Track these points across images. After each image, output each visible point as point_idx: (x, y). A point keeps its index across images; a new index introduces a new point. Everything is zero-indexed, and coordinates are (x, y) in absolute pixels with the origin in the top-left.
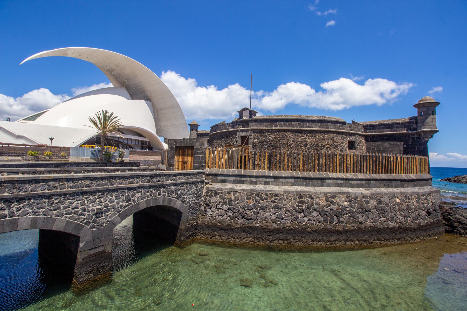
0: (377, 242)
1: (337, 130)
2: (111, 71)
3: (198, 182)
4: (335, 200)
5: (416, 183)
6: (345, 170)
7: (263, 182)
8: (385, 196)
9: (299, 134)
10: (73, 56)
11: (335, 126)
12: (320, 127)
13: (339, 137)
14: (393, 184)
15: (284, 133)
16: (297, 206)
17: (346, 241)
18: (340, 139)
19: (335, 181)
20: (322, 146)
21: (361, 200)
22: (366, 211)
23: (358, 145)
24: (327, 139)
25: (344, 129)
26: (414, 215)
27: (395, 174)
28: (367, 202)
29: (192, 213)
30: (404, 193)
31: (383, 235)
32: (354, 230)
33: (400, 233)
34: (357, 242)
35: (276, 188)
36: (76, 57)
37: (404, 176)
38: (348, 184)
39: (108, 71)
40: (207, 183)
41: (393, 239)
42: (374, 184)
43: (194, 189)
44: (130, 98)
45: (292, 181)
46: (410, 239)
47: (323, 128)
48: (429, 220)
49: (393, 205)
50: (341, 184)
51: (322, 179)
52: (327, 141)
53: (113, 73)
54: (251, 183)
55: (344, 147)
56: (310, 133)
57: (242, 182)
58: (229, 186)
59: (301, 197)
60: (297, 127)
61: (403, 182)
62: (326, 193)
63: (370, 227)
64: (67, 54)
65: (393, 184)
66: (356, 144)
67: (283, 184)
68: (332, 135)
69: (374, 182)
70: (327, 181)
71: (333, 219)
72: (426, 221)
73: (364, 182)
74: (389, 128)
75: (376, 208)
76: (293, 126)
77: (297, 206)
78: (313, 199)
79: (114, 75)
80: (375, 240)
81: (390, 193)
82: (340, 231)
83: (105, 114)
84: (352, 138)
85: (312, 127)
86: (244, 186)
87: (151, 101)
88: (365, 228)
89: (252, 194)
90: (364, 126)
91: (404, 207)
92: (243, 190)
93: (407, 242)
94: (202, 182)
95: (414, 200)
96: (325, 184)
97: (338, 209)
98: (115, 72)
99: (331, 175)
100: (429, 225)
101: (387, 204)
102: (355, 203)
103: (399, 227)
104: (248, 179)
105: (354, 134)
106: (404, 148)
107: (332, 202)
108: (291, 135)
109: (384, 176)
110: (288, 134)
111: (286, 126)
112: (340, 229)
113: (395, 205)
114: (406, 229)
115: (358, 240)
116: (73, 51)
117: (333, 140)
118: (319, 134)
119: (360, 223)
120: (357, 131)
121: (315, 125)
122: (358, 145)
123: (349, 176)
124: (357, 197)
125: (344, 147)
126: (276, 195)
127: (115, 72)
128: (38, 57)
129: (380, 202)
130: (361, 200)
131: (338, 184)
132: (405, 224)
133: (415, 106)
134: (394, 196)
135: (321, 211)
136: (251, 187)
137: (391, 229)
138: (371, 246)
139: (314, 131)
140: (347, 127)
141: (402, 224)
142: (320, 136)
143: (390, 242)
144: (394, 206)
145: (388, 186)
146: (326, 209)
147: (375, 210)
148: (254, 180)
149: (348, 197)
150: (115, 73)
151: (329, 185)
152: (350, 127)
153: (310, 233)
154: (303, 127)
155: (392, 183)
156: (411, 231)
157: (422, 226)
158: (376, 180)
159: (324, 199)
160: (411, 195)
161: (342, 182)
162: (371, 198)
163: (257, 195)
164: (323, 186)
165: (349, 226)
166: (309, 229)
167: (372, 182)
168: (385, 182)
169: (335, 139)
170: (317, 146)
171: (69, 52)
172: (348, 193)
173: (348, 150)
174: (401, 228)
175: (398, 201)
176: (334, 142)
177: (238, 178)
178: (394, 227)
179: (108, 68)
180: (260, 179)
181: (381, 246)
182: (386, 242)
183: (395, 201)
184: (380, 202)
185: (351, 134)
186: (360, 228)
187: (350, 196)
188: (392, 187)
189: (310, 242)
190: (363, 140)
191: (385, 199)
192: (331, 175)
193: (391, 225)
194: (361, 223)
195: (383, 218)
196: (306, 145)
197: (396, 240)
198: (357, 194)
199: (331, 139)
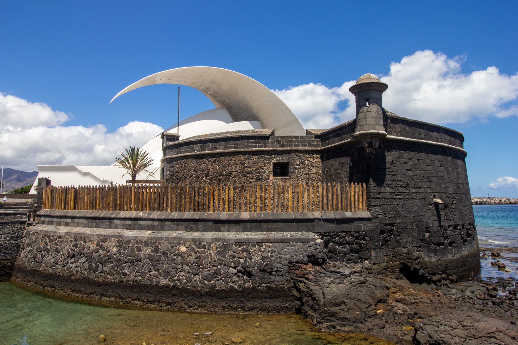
0: (137, 302)
1: (250, 149)
2: (206, 90)
3: (14, 223)
4: (105, 245)
5: (270, 225)
7: (64, 223)
8: (166, 243)
9: (200, 161)
10: (162, 82)
11: (248, 143)
12: (225, 148)
13: (255, 159)
14: (200, 226)
15: (185, 160)
16: (71, 249)
17: (102, 295)
18: (257, 163)
19: (123, 222)
20: (227, 175)
21: (133, 245)
22: (134, 261)
23: (296, 169)
24: (234, 164)
25: (266, 146)
26: (206, 273)
27: (211, 212)
28: (139, 250)
29: (4, 253)
30: (199, 239)
31: (147, 295)
32: (113, 283)
33: (174, 295)
34: (113, 299)
35: (63, 230)
36: (166, 83)
37: (224, 215)
38: (137, 226)
39: (204, 90)
40: (30, 225)
41: (159, 302)
42: (170, 226)
43: (8, 229)
44: (231, 119)
45: (84, 221)
46: (186, 307)
47: (230, 148)
48: (238, 282)
49: (174, 255)
50: (130, 225)
51: (111, 219)
52: (234, 167)
53: (209, 93)
55: (264, 173)
56: (213, 157)
59: (76, 240)
60: (198, 150)
61: (218, 224)
62: (99, 236)
63: (133, 282)
64: (156, 81)
65: (200, 226)
66: (291, 169)
68: (242, 158)
69: (169, 223)
70: (116, 222)
71: (97, 267)
72: (231, 284)
73: (156, 223)
74: (339, 135)
75: (150, 257)
76: (194, 151)
77: (71, 249)
79: (210, 94)
80: (135, 300)
81: (175, 239)
82: (99, 282)
83: (133, 149)
84: (283, 159)
85: (215, 149)
87: (259, 121)
88: (127, 282)
89: (45, 235)
90: (317, 137)
91: (193, 258)
93: (180, 310)
94: (23, 223)
95: (213, 252)
96: (113, 225)
97: (105, 255)
98: (212, 91)
99: (123, 214)
100: (236, 291)
101: (164, 253)
102: (125, 249)
103: (174, 286)
105: (289, 152)
106: (350, 167)
107: (102, 247)
108: (192, 162)
109: (188, 215)
110: (189, 161)
111: (188, 152)
112: (100, 280)
113: (177, 255)
114: (186, 291)
115: (114, 296)
116: (161, 76)
117: (243, 164)
118: (223, 158)
119: (123, 275)
120: (296, 146)
121: (220, 146)
122: (296, 169)
123: (141, 214)
124: (129, 242)
125: (264, 173)
126: (60, 237)
127: (212, 91)
128: (127, 92)
129: (157, 250)
130: (133, 245)
131: (125, 225)
132: (185, 283)
134: (179, 242)
135: (90, 258)
137: (162, 287)
138: (127, 306)
139: (217, 154)
140: (272, 143)
141: (181, 283)
142: (224, 160)
143: (152, 306)
144: (175, 257)
145: (192, 229)
146: (95, 255)
147: (148, 260)
149: (119, 241)
150: (211, 92)
152: (278, 142)
153: (73, 281)
154: (205, 150)
155: (197, 225)
156: (193, 295)
157: (218, 291)
158: (172, 220)
159: (95, 243)
160: (209, 243)
161: (129, 222)
162: (146, 244)
164: (110, 228)
165: (111, 277)
166: (73, 278)
167: (167, 223)
168: (186, 224)
169: (246, 163)
170: (221, 175)
171: (157, 78)
173: (271, 177)
174: (177, 289)
175: (183, 249)
176: (245, 167)
178: (166, 286)
179: (202, 87)
181: (141, 308)
182: (149, 305)
183: (178, 249)
184: (157, 250)
185: (280, 153)
186: (122, 282)
187: (121, 241)
188: (197, 230)
189: (69, 292)
190: (317, 159)
191: (164, 247)
192: (123, 214)
193: (164, 282)
194: (125, 275)
195: (154, 272)
196: (207, 175)
197: (164, 305)
198: (130, 238)
199: (240, 163)
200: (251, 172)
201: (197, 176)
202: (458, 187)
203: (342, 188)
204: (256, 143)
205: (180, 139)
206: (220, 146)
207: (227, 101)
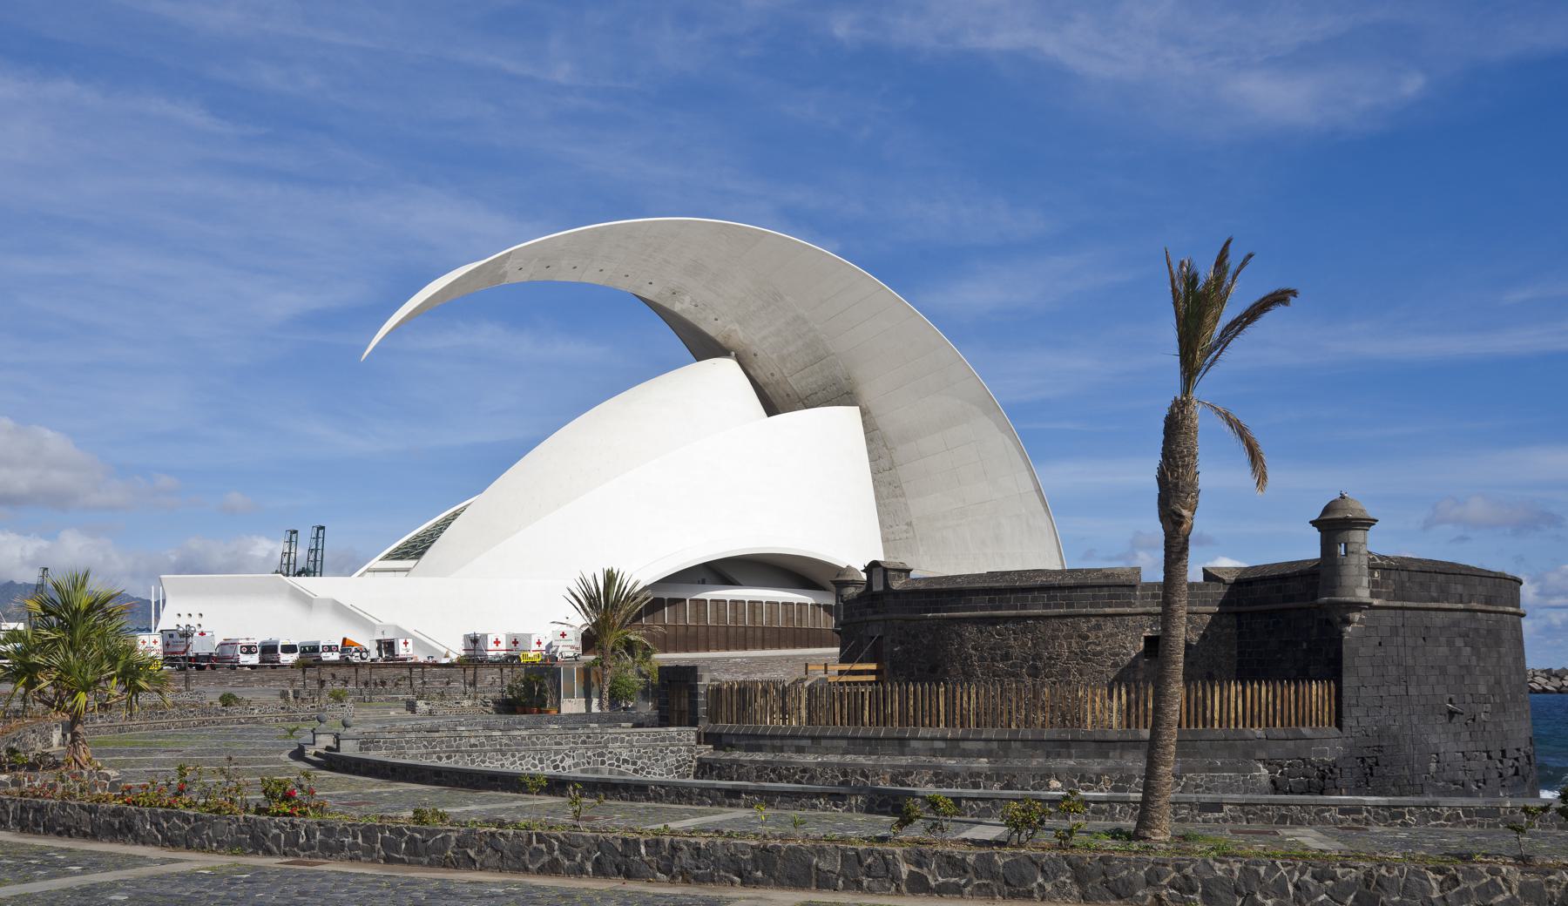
6: (958, 722)
12: (1046, 606)
20: (1050, 658)
45: (844, 743)
54: (774, 749)
57: (759, 749)
58: (736, 755)
59: (845, 774)
67: (828, 751)
70: (914, 744)
76: (974, 609)
78: (867, 777)
85: (1024, 607)
86: (759, 757)
92: (752, 762)
104: (768, 742)
108: (970, 632)
126: (804, 771)
133: (1314, 523)
136: (770, 757)
148: (777, 743)
151: (914, 753)
154: (999, 608)
163: (773, 771)
170: (1038, 657)
172: (939, 767)
177: (753, 742)
180: (789, 742)
200: (1101, 653)
201: (982, 659)
202: (1498, 682)
203: (1296, 692)
204: (1111, 597)
205: (913, 575)
206: (1034, 599)
207: (741, 335)
